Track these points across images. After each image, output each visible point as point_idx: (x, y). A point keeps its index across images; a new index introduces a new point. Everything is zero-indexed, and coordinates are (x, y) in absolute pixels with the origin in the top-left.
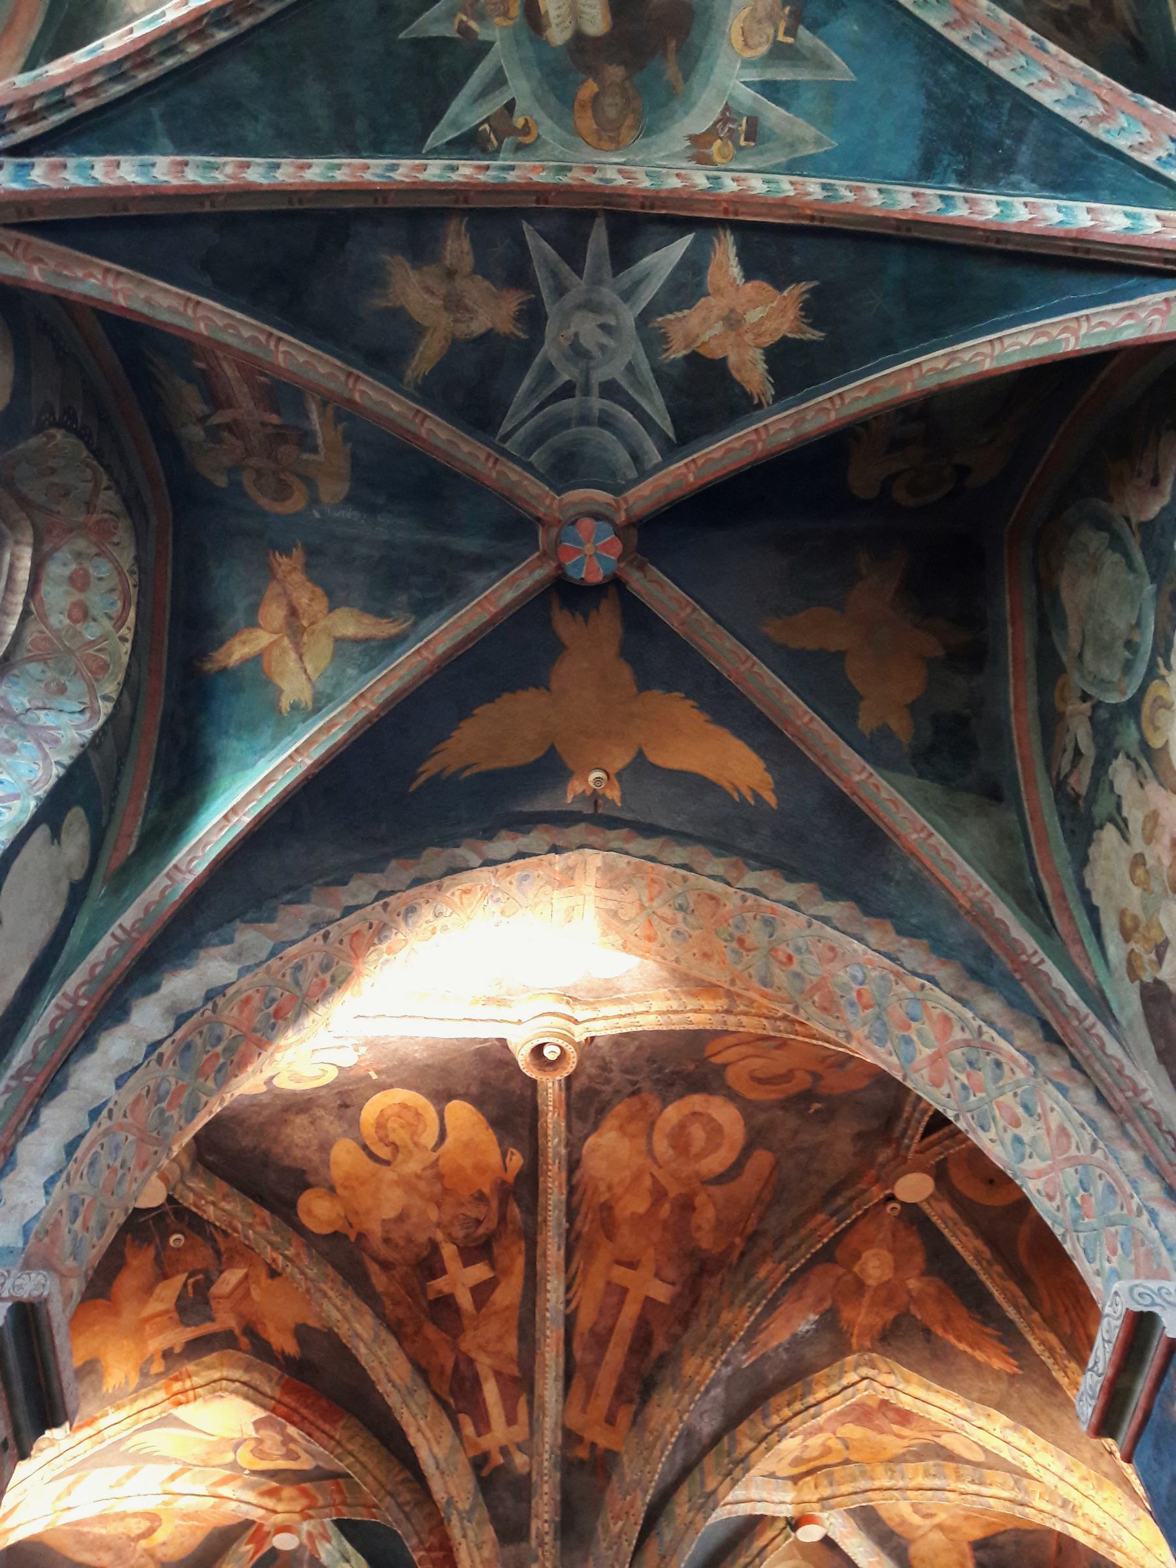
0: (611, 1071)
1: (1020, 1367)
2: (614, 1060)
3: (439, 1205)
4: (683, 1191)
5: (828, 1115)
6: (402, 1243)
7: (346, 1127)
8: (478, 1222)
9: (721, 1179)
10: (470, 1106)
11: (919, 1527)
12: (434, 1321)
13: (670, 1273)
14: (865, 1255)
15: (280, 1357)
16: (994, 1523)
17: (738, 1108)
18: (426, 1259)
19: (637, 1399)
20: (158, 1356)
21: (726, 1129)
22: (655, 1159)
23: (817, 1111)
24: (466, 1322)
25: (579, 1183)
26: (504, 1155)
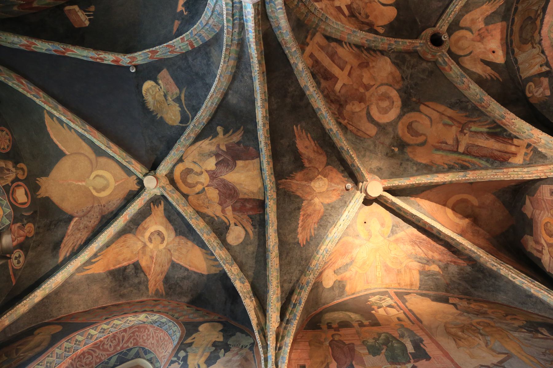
0: (412, 69)
1: (304, 245)
2: (416, 70)
4: (367, 99)
5: (390, 155)
9: (368, 114)
10: (396, 15)
11: (143, 237)
13: (343, 91)
14: (325, 179)
16: (150, 270)
19: (312, 70)
21: (386, 115)
23: (393, 150)
25: (377, 54)
26: (382, 26)
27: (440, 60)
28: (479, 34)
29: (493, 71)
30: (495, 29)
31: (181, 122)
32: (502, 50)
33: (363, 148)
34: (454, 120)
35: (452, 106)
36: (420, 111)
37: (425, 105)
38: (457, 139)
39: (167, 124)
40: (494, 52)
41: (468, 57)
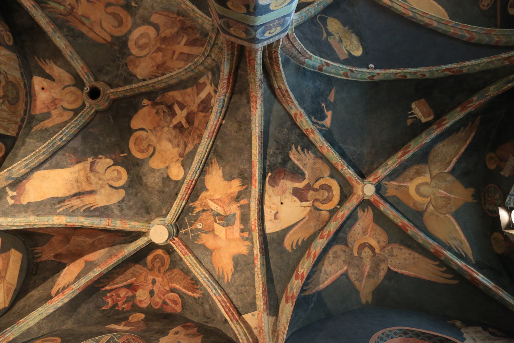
2: (114, 73)
3: (163, 128)
4: (159, 42)
6: (177, 140)
7: (145, 164)
8: (164, 112)
12: (193, 124)
13: (181, 38)
15: (244, 187)
17: (134, 30)
18: (179, 130)
20: (242, 233)
21: (142, 32)
22: (148, 54)
23: (136, 3)
24: (190, 110)
26: (144, 106)
27: (92, 79)
28: (56, 105)
29: (44, 68)
30: (42, 108)
31: (328, 18)
32: (35, 90)
33: (163, 3)
34: (79, 21)
35: (82, 35)
36: (112, 36)
37: (106, 40)
38: (77, 3)
39: (339, 20)
40: (43, 89)
41: (67, 84)
